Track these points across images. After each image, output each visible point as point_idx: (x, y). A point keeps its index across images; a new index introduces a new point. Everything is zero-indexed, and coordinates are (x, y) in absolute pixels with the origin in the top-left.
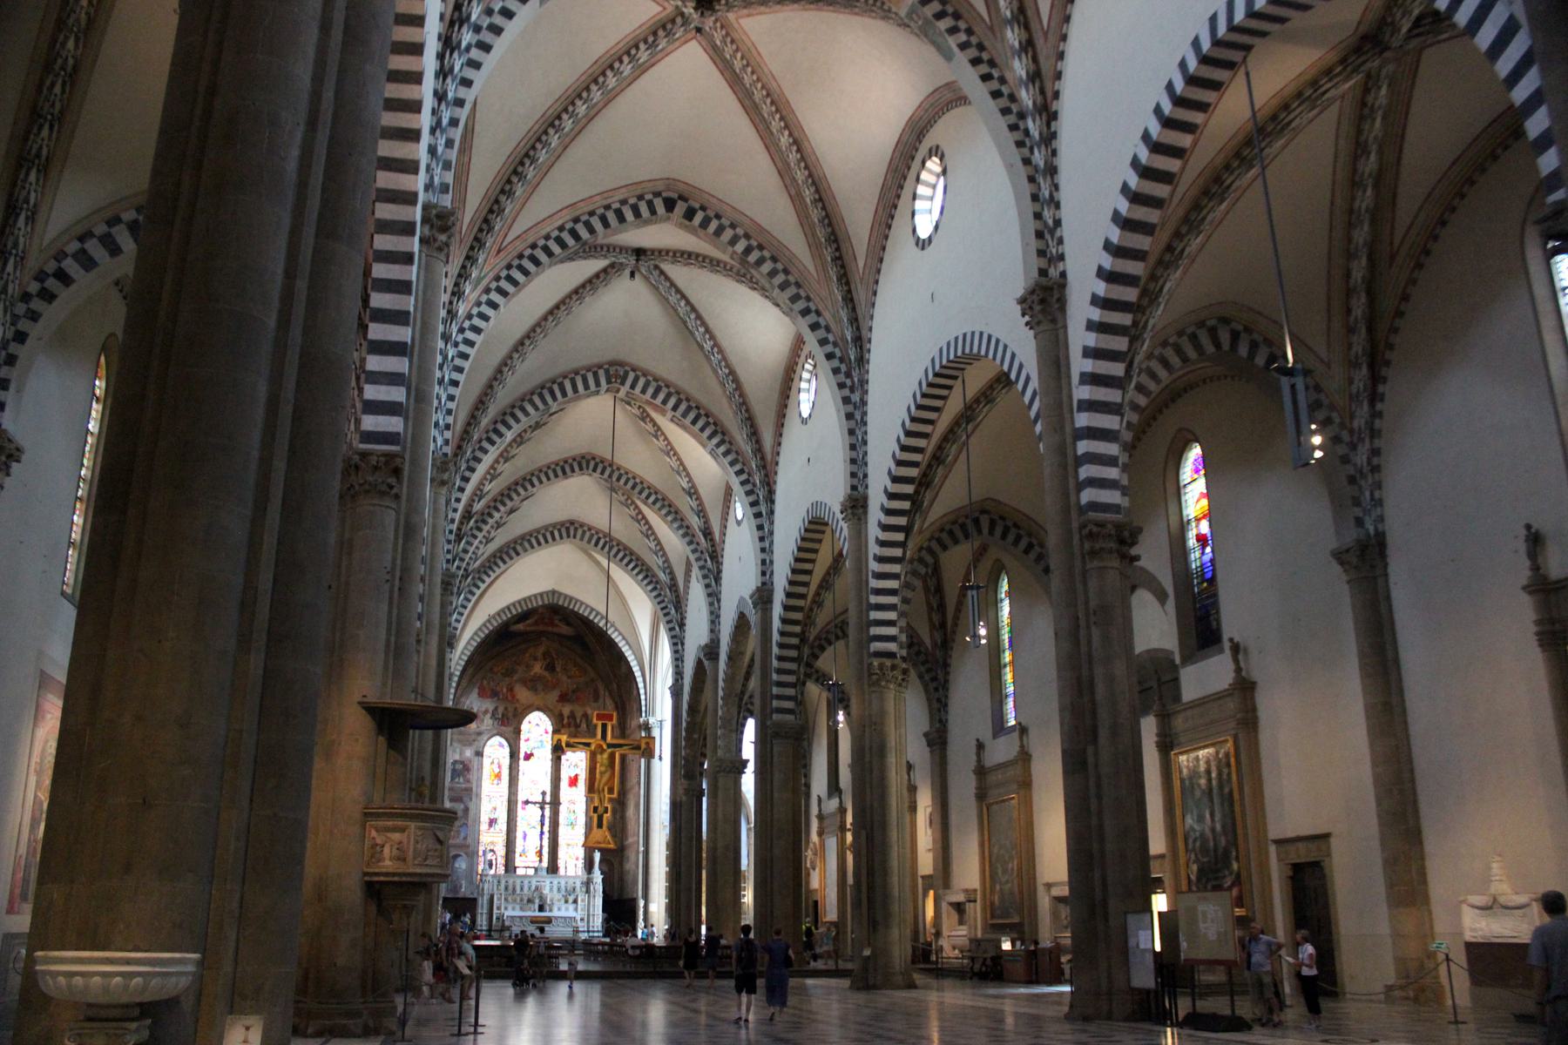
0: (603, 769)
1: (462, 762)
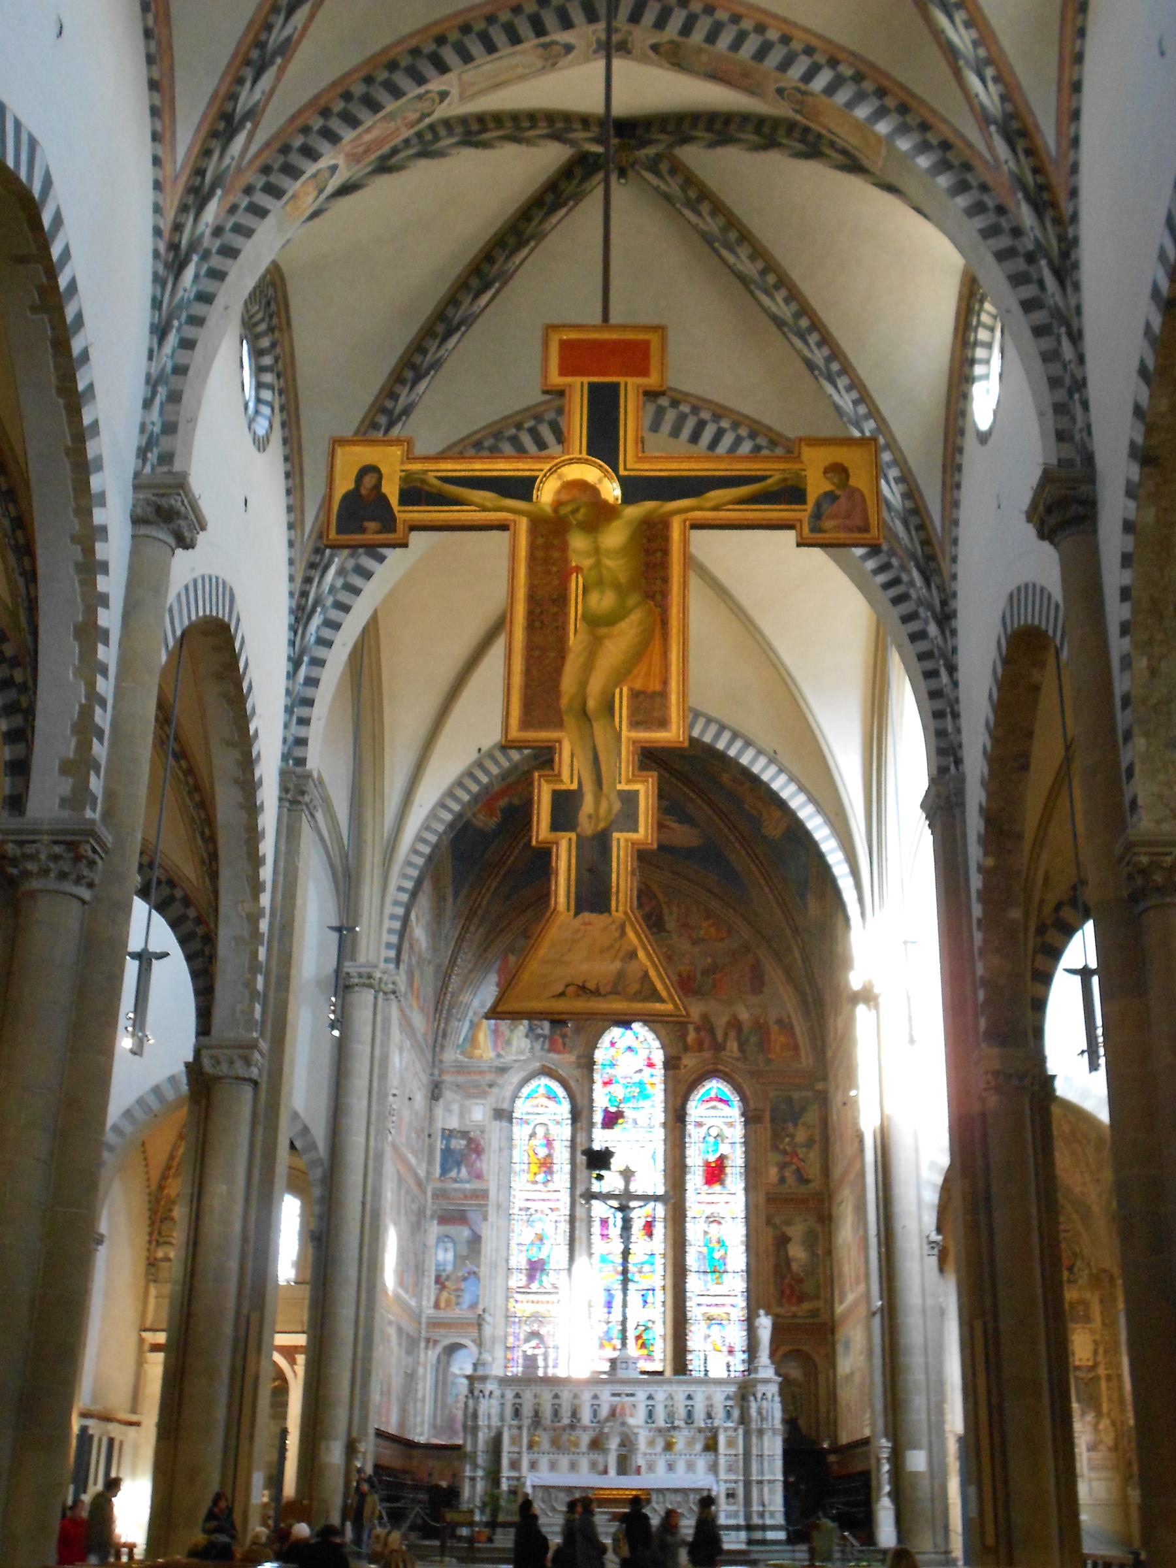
0: (602, 601)
1: (465, 1134)
